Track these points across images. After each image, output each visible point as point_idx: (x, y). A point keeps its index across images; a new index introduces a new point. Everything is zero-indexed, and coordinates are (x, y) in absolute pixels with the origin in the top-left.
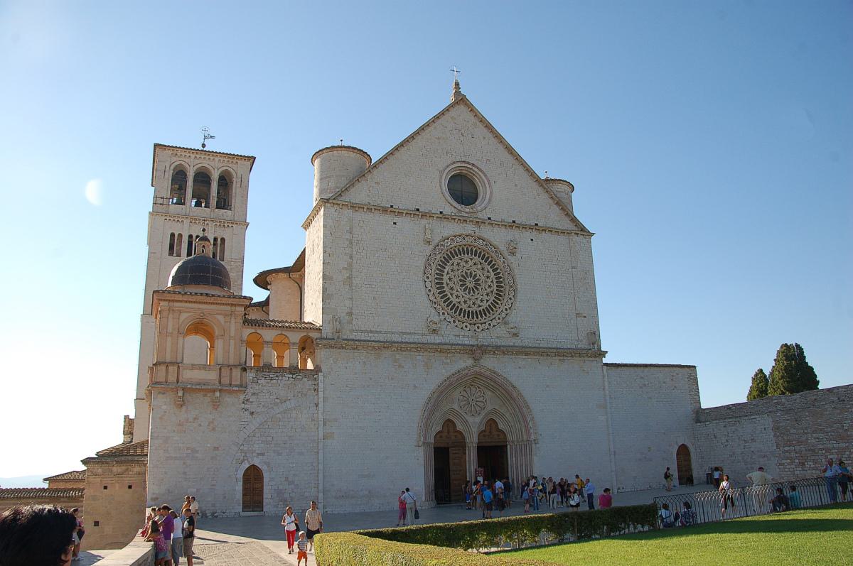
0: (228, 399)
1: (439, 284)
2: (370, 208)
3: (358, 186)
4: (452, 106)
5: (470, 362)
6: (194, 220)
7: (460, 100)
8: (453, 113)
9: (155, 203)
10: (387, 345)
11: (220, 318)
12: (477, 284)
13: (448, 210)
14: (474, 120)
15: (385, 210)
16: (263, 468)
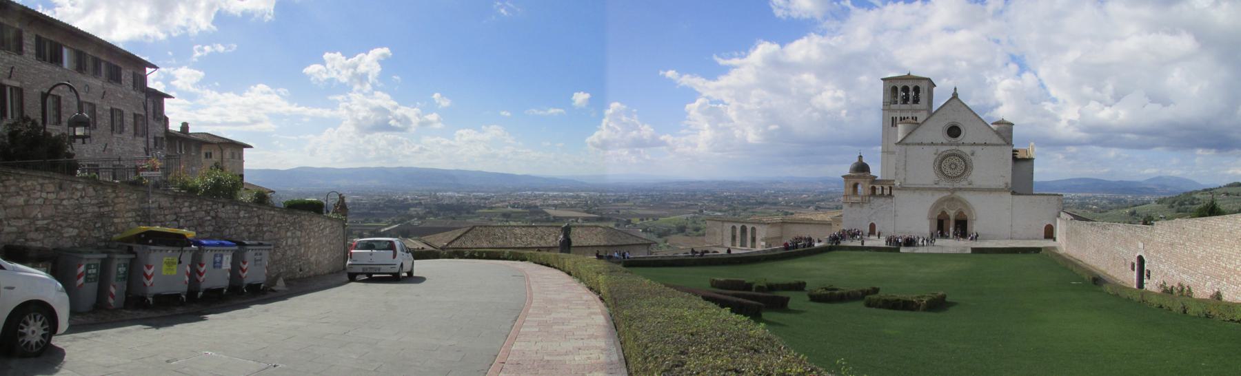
0: (865, 205)
1: (940, 167)
2: (913, 144)
3: (909, 136)
4: (951, 99)
5: (949, 194)
6: (902, 111)
7: (955, 96)
8: (950, 103)
9: (884, 105)
10: (917, 189)
11: (862, 182)
12: (956, 166)
13: (945, 141)
14: (959, 104)
15: (918, 144)
16: (875, 223)
